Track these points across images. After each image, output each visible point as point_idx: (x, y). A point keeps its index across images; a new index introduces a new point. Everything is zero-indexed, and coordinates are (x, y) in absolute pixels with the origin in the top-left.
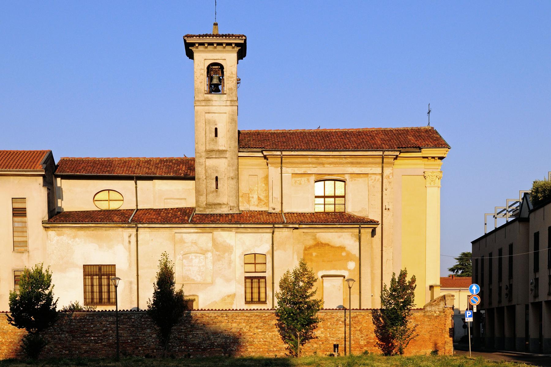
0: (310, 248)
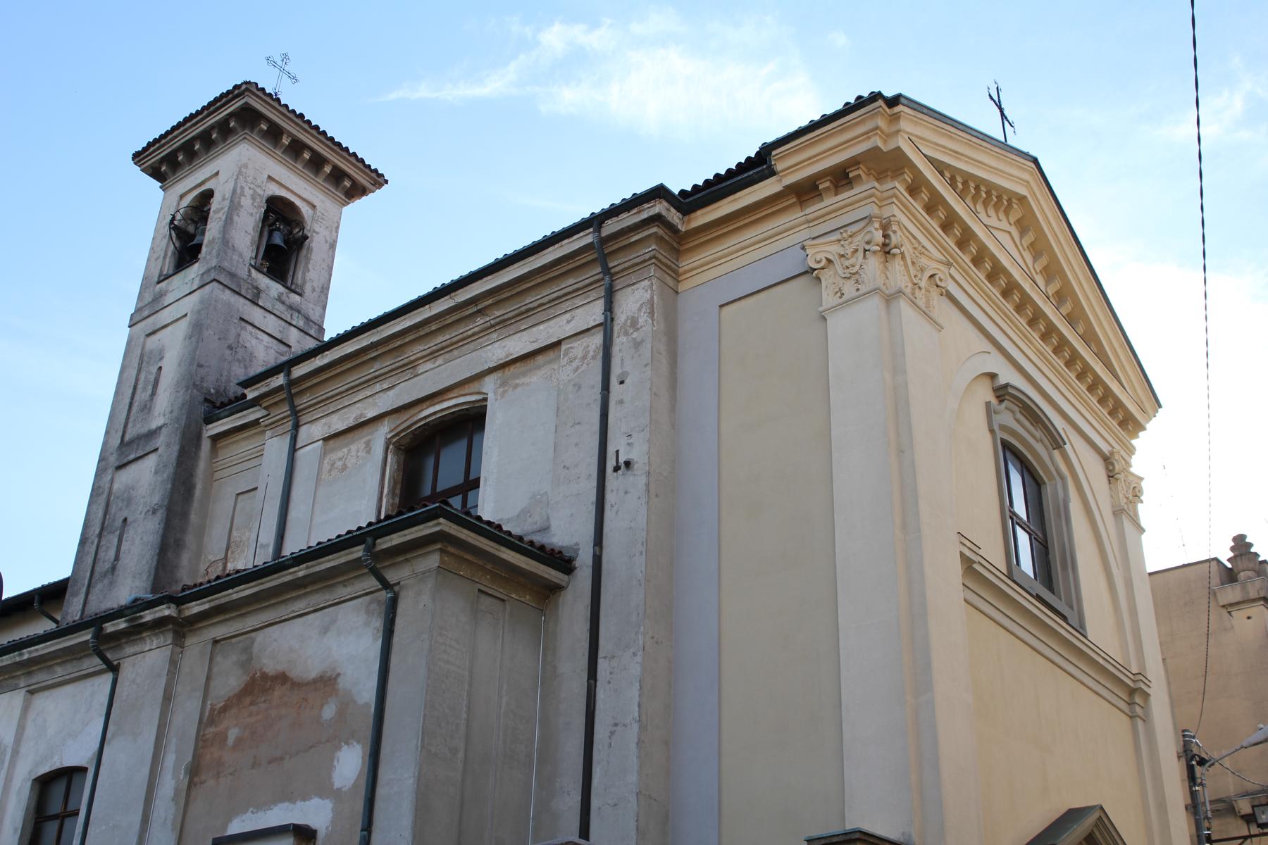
0: (224, 709)
